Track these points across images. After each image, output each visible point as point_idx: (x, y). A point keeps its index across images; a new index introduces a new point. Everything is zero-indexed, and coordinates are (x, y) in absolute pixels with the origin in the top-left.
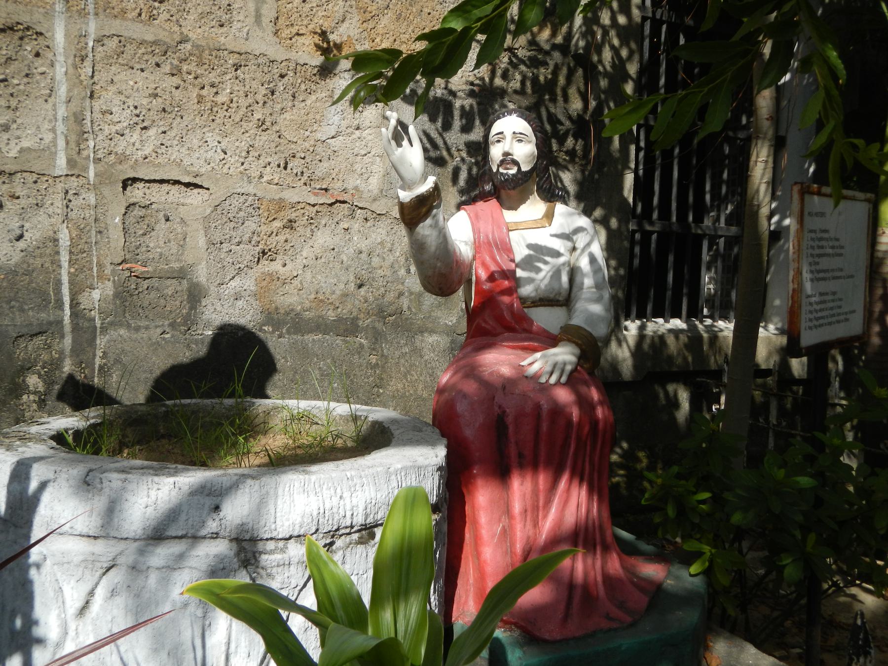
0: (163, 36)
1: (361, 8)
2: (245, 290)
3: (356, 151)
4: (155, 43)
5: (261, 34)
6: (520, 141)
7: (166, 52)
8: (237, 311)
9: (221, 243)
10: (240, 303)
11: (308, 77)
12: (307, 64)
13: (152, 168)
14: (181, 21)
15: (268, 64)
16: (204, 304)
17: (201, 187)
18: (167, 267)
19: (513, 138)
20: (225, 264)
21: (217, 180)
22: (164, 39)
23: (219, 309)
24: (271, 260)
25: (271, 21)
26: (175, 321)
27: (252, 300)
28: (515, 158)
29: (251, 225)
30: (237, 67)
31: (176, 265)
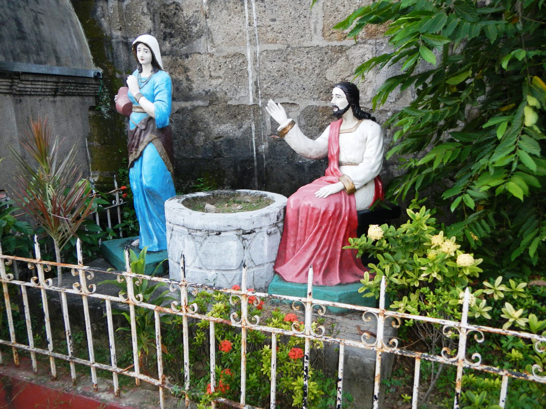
4: (278, 50)
5: (316, 37)
14: (288, 39)
29: (315, 118)
30: (308, 53)
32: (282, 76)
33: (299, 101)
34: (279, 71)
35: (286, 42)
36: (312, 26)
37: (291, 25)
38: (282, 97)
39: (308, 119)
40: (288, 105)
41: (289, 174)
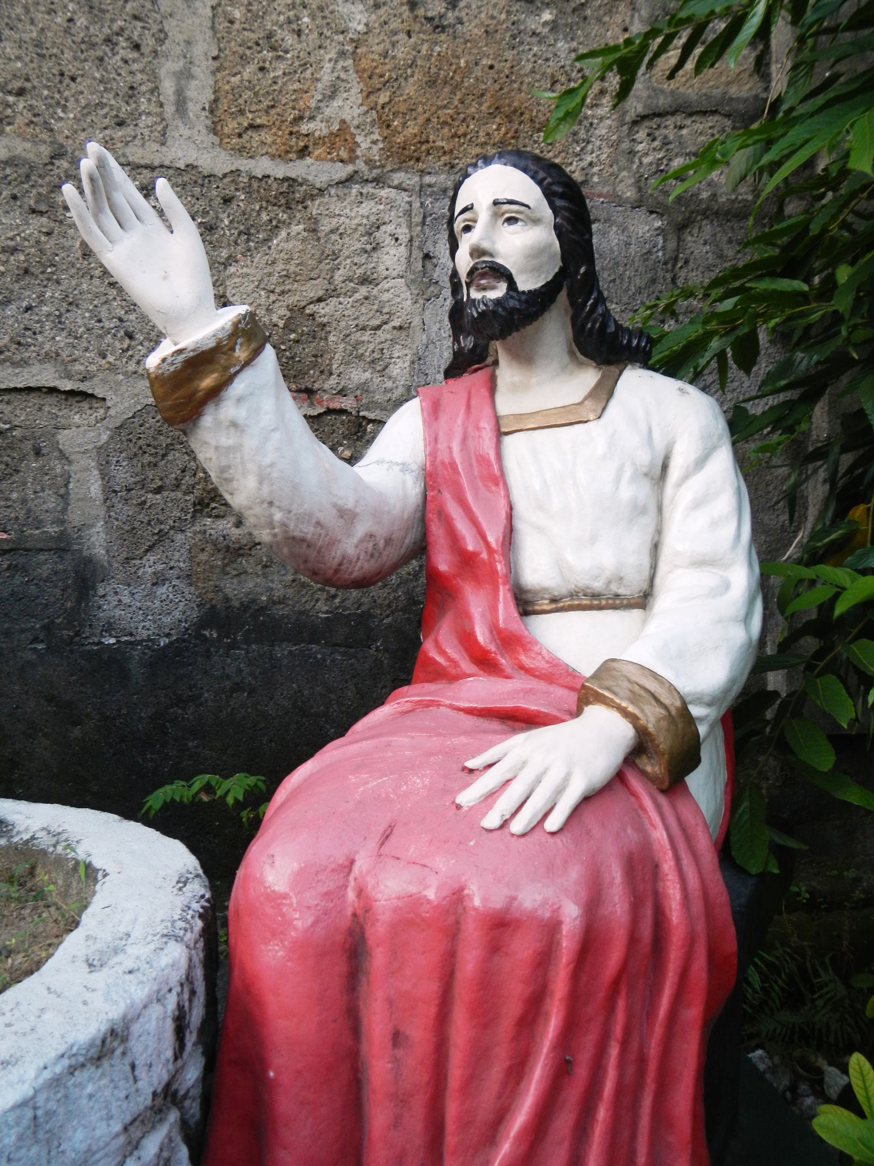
0: (22, 148)
1: (364, 70)
2: (171, 568)
3: (361, 321)
5: (186, 132)
6: (511, 220)
7: (28, 176)
8: (157, 603)
9: (129, 490)
10: (162, 591)
11: (271, 199)
12: (268, 177)
13: (10, 370)
14: (56, 126)
15: (200, 181)
16: (101, 592)
17: (92, 396)
18: (37, 532)
19: (496, 215)
20: (137, 524)
21: (119, 383)
22: (24, 154)
23: (126, 600)
24: (217, 517)
25: (204, 109)
26: (53, 622)
27: (181, 584)
28: (500, 261)
31: (52, 530)
32: (26, 271)
33: (104, 381)
34: (14, 250)
35: (45, 136)
36: (168, 87)
37: (70, 69)
38: (25, 363)
39: (147, 459)
40: (52, 399)
41: (50, 699)
